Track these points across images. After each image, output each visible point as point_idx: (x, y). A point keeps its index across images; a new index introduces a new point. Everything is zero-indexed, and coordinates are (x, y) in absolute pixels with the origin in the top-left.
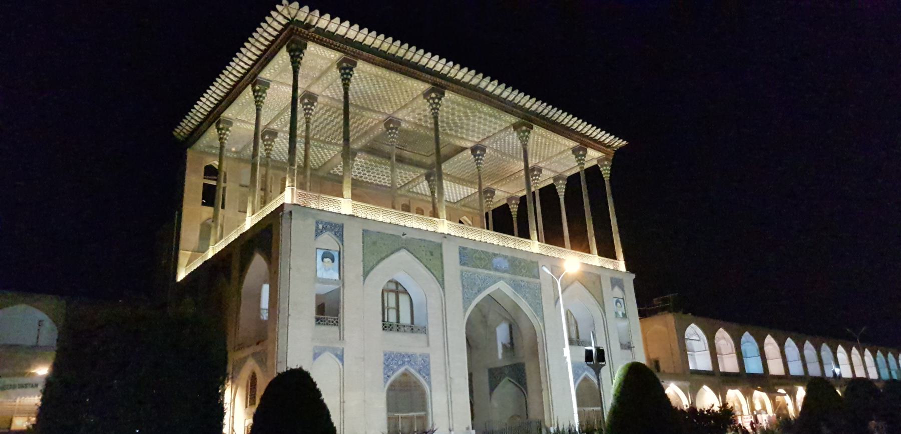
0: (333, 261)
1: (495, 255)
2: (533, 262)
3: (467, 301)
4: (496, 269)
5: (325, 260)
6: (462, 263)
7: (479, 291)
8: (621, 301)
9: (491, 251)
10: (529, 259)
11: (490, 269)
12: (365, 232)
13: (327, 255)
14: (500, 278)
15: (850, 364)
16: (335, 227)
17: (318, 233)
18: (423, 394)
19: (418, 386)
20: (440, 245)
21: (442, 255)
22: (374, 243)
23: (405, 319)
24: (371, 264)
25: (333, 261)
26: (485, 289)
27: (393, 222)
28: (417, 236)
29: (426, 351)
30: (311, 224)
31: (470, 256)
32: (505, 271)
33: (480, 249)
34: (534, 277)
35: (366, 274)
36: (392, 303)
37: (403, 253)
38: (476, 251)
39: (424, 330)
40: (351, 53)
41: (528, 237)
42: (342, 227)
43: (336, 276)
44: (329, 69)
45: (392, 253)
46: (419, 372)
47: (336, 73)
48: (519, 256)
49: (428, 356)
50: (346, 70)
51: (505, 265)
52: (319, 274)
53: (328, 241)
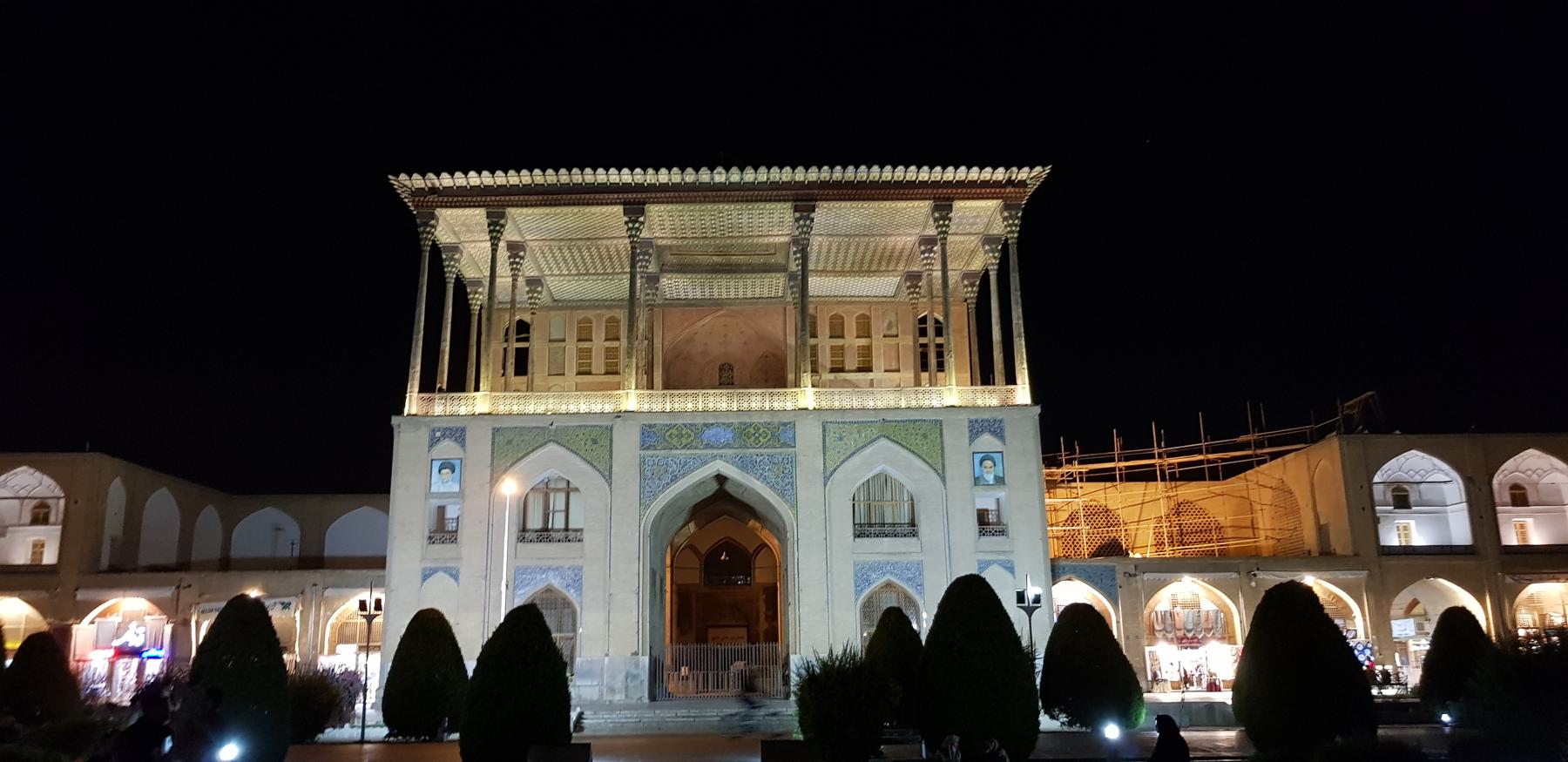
1: (706, 425)
2: (785, 424)
3: (645, 499)
4: (708, 446)
6: (644, 447)
7: (674, 479)
9: (699, 421)
10: (776, 420)
12: (496, 431)
13: (447, 465)
14: (714, 457)
15: (1039, 664)
16: (457, 432)
17: (434, 441)
18: (574, 612)
19: (567, 604)
22: (509, 442)
26: (684, 476)
29: (579, 562)
30: (424, 435)
31: (653, 434)
32: (727, 446)
33: (680, 422)
36: (561, 505)
37: (552, 447)
40: (496, 203)
42: (463, 430)
43: (456, 488)
48: (756, 419)
50: (495, 228)
52: (434, 489)
53: (447, 448)
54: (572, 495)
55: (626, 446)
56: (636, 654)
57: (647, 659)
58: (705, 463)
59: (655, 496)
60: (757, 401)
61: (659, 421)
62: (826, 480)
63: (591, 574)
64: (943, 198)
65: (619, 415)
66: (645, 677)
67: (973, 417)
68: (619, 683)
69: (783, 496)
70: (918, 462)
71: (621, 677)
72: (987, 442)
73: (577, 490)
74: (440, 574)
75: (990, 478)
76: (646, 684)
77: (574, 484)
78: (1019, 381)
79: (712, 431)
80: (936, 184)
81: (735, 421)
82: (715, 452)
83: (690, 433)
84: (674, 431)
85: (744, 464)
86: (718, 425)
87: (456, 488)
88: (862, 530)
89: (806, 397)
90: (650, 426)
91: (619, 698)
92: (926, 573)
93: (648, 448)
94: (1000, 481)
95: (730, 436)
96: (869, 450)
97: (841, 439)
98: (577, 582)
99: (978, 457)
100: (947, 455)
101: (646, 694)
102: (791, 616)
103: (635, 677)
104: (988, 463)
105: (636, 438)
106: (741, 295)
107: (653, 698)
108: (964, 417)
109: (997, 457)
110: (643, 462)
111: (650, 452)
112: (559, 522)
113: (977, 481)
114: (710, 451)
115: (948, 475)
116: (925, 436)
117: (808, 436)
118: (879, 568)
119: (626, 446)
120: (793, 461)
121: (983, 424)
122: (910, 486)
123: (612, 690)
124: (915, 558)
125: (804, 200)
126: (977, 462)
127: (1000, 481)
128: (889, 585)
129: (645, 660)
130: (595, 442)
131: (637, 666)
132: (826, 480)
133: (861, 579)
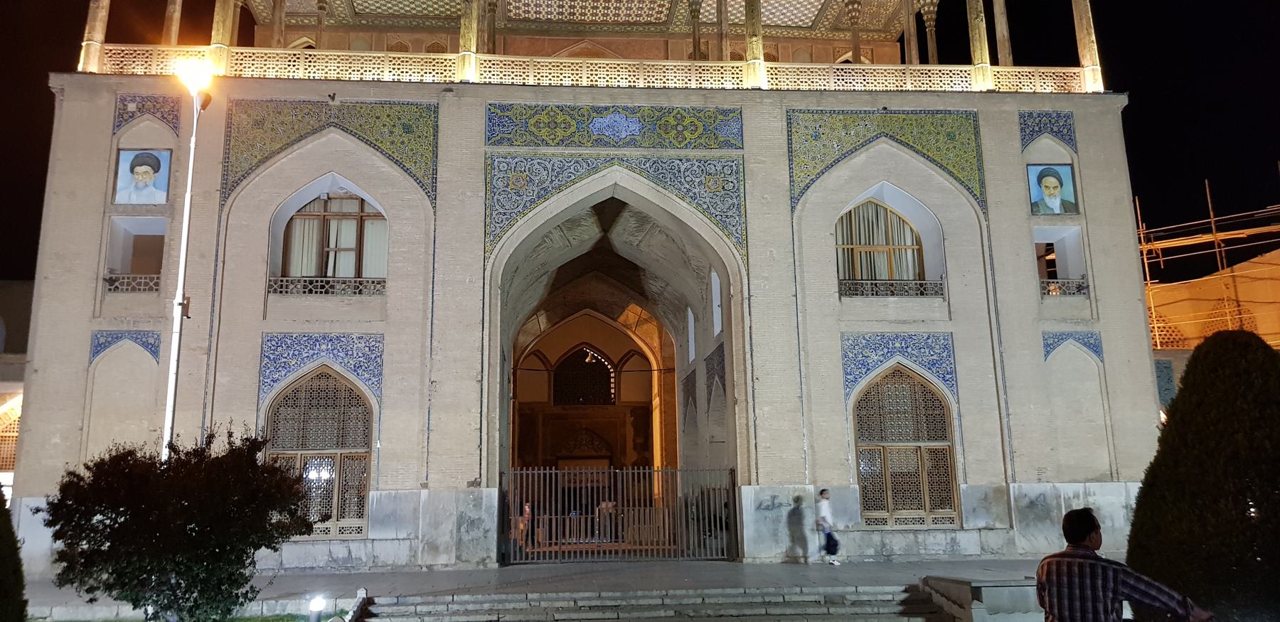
0: (156, 168)
1: (599, 111)
2: (725, 112)
4: (599, 142)
5: (138, 169)
6: (492, 138)
7: (544, 195)
8: (1065, 172)
9: (585, 101)
10: (711, 106)
11: (581, 144)
13: (147, 159)
14: (610, 161)
17: (122, 119)
19: (356, 399)
20: (436, 109)
21: (436, 128)
23: (909, 273)
24: (246, 166)
25: (156, 168)
26: (559, 189)
28: (371, 97)
29: (376, 328)
30: (105, 105)
32: (632, 143)
33: (553, 102)
34: (727, 144)
35: (228, 188)
37: (334, 137)
38: (537, 110)
39: (939, 291)
41: (968, 61)
43: (160, 198)
45: (301, 138)
46: (356, 368)
48: (678, 103)
49: (380, 339)
51: (631, 127)
52: (121, 198)
54: (369, 226)
55: (462, 142)
56: (476, 483)
57: (495, 492)
58: (596, 170)
59: (510, 219)
61: (519, 100)
62: (794, 201)
63: (399, 354)
65: (449, 87)
66: (492, 523)
67: (1026, 109)
68: (445, 534)
69: (722, 223)
70: (940, 178)
71: (449, 526)
72: (1048, 148)
73: (378, 216)
74: (127, 344)
75: (1055, 204)
76: (494, 535)
77: (374, 203)
78: (1084, 62)
79: (608, 119)
81: (643, 102)
82: (612, 152)
83: (573, 122)
85: (660, 174)
86: (616, 110)
87: (160, 198)
88: (853, 283)
90: (503, 108)
91: (444, 560)
92: (959, 354)
93: (500, 142)
94: (1071, 208)
95: (635, 127)
96: (860, 158)
97: (816, 137)
98: (372, 362)
99: (1034, 172)
100: (987, 166)
101: (494, 555)
102: (740, 422)
103: (473, 523)
104: (1051, 181)
105: (478, 124)
107: (503, 559)
108: (1012, 109)
109: (1065, 172)
110: (489, 165)
111: (503, 149)
112: (344, 267)
113: (1035, 208)
114: (604, 152)
115: (991, 197)
116: (951, 137)
117: (764, 135)
118: (884, 343)
119: (462, 142)
120: (738, 170)
121: (1037, 123)
122: (917, 220)
123: (433, 548)
124: (942, 327)
126: (1033, 179)
127: (1071, 208)
128: (898, 373)
129: (492, 495)
130: (407, 129)
131: (478, 503)
132: (794, 201)
133: (854, 362)
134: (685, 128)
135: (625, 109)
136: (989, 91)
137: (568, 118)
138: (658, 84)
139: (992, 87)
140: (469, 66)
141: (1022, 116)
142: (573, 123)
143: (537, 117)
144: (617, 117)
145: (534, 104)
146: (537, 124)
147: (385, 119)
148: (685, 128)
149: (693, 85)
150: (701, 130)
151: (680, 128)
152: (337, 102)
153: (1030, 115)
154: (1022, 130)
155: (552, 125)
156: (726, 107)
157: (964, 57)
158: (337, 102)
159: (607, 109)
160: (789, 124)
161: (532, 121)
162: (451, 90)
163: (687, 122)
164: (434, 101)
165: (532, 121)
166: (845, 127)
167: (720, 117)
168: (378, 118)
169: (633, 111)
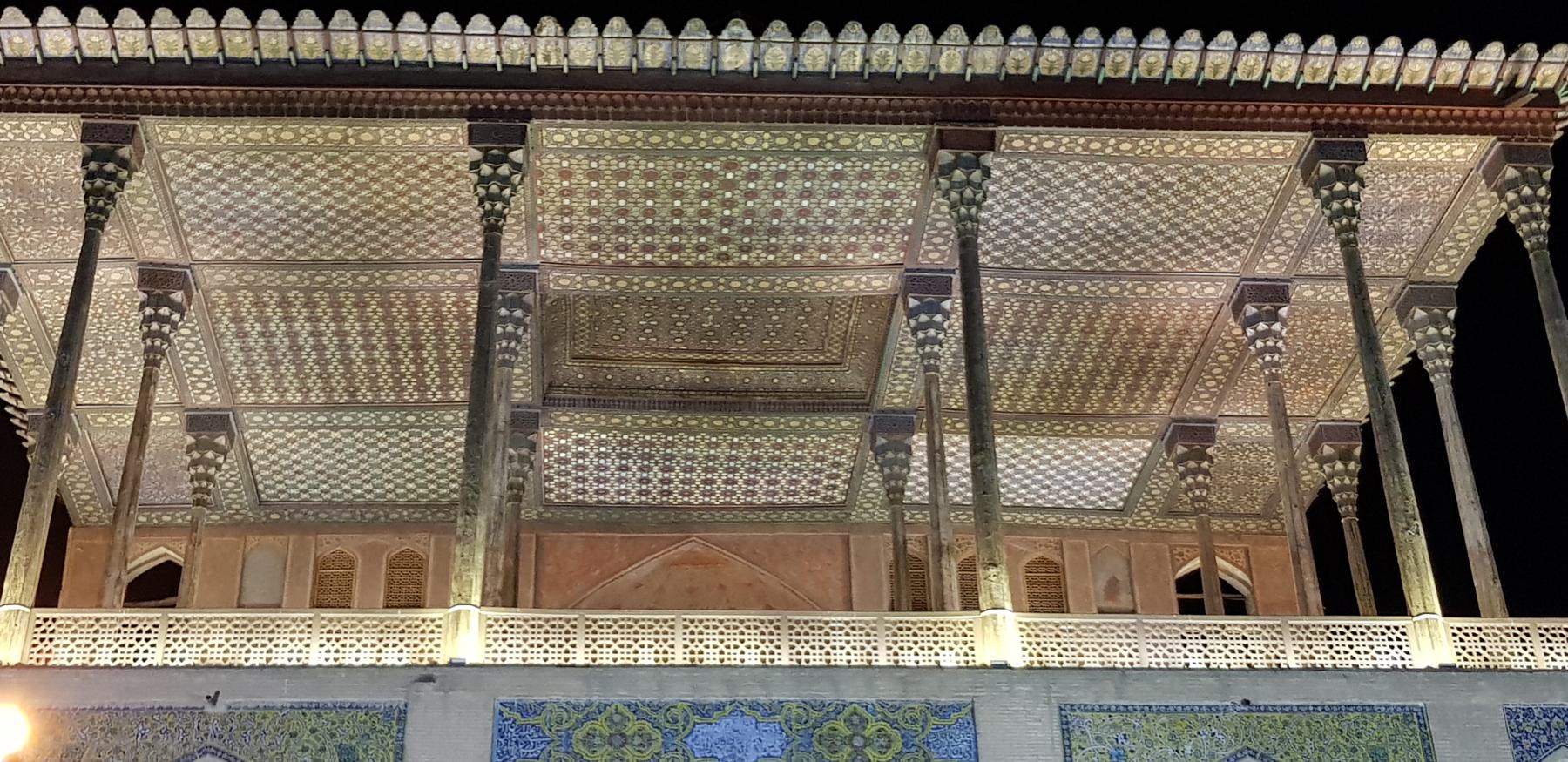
1: (703, 711)
2: (942, 711)
9: (679, 694)
10: (916, 699)
27: (216, 656)
28: (284, 696)
38: (588, 713)
44: (1282, 198)
47: (1306, 202)
48: (854, 694)
60: (861, 646)
61: (554, 694)
64: (1338, 128)
65: (428, 674)
67: (1518, 701)
80: (1316, 92)
84: (602, 727)
86: (737, 708)
89: (1002, 635)
90: (525, 710)
106: (739, 499)
108: (1491, 698)
125: (964, 120)
134: (868, 742)
135: (754, 706)
136: (1447, 668)
137: (647, 726)
138: (817, 659)
139: (1451, 659)
140: (466, 633)
141: (1511, 714)
142: (657, 735)
143: (587, 726)
144: (739, 725)
145: (583, 700)
146: (588, 740)
147: (305, 736)
148: (868, 742)
149: (882, 659)
150: (898, 746)
151: (858, 742)
152: (220, 708)
153: (1528, 713)
154: (1516, 742)
155: (617, 741)
156: (943, 700)
157: (1393, 602)
158: (220, 708)
159: (719, 707)
160: (1066, 731)
161: (580, 734)
162: (430, 679)
163: (871, 730)
164: (398, 700)
165: (580, 734)
166: (1173, 738)
167: (934, 720)
168: (293, 735)
169: (771, 710)
